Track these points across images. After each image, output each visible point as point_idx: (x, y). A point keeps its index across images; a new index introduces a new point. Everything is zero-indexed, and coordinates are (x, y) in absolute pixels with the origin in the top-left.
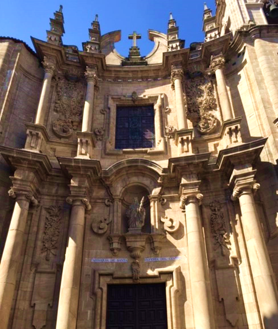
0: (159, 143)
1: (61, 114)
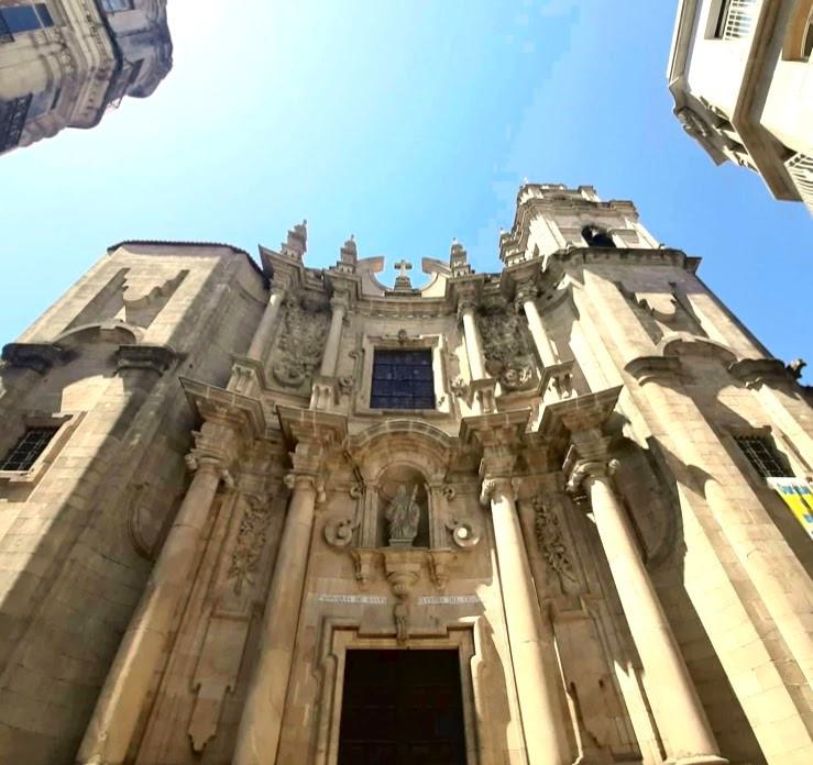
0: (440, 403)
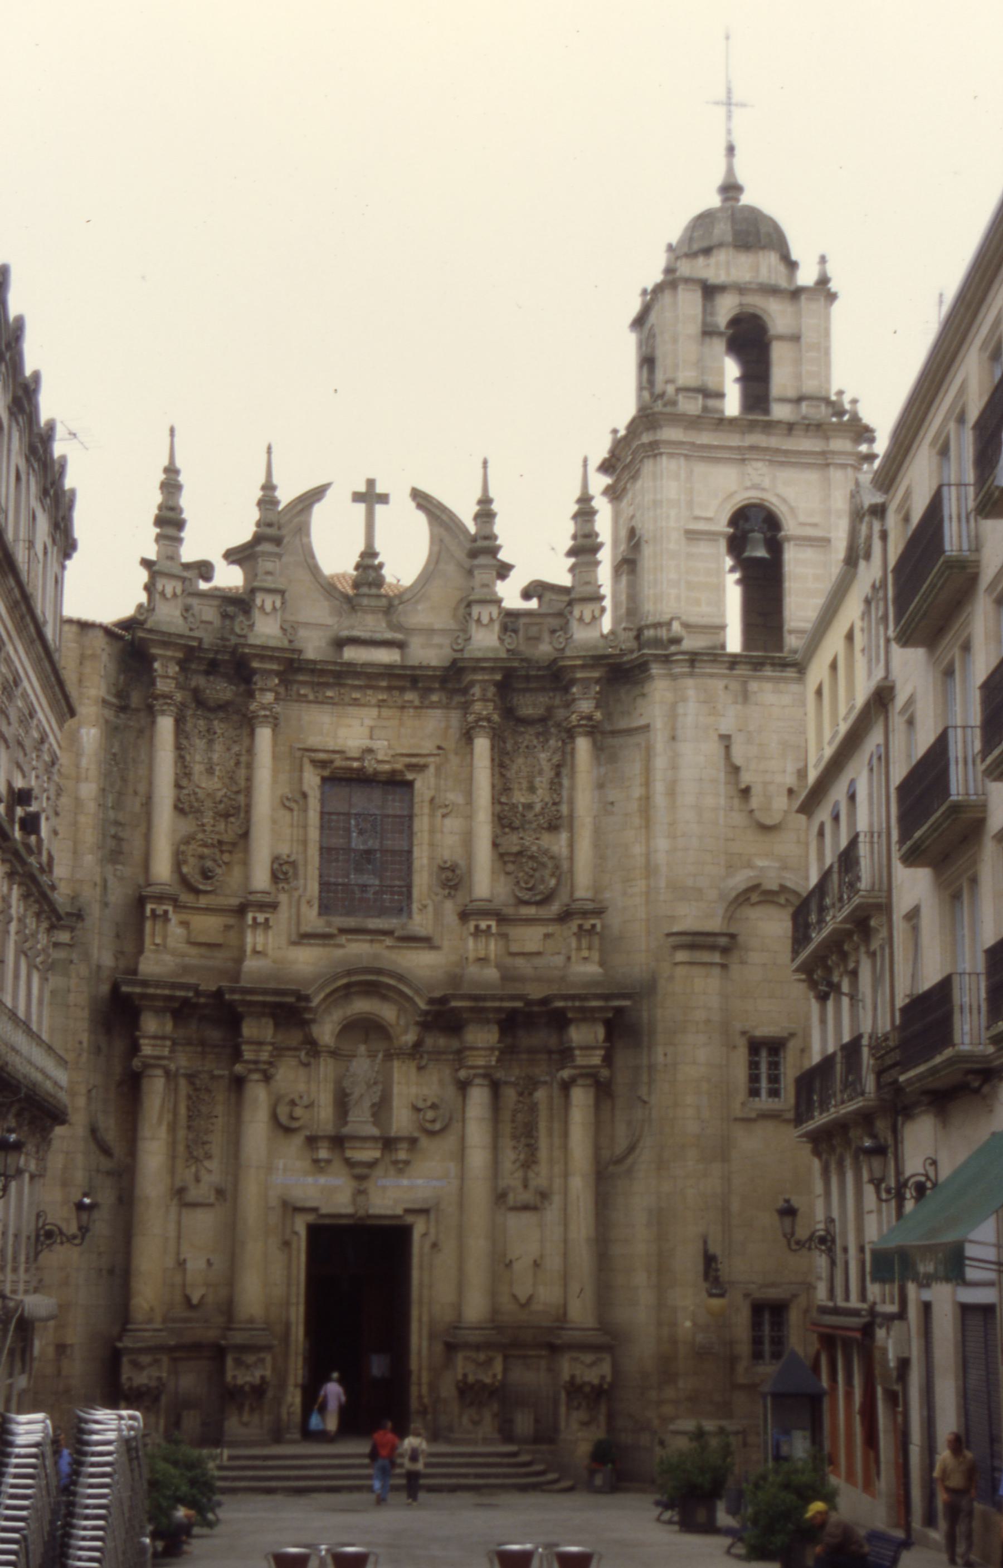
1: (191, 816)
